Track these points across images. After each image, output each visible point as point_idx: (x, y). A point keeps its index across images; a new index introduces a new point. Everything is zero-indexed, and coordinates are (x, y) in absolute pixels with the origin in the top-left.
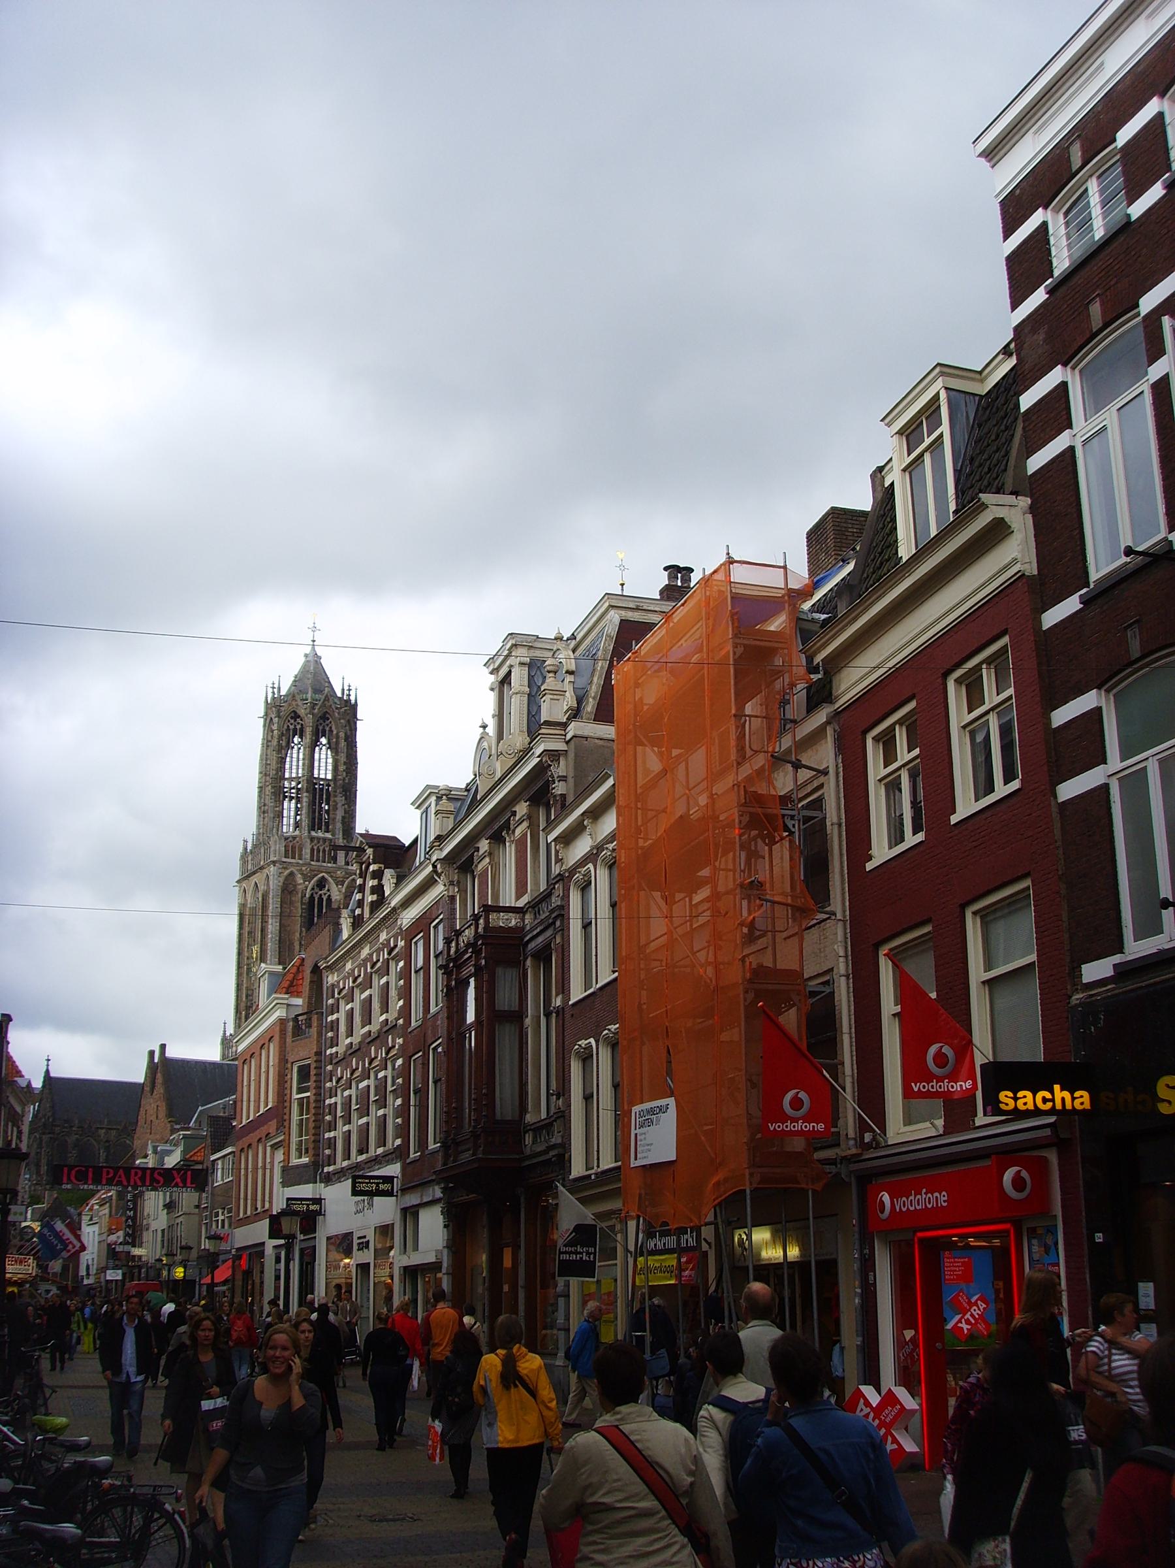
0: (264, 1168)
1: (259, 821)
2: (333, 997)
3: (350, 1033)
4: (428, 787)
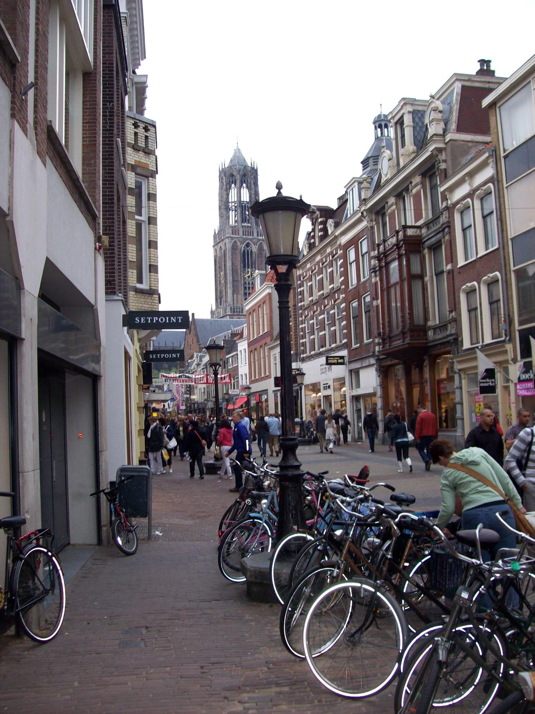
0: (264, 358)
1: (220, 220)
2: (300, 280)
3: (311, 295)
4: (354, 178)
